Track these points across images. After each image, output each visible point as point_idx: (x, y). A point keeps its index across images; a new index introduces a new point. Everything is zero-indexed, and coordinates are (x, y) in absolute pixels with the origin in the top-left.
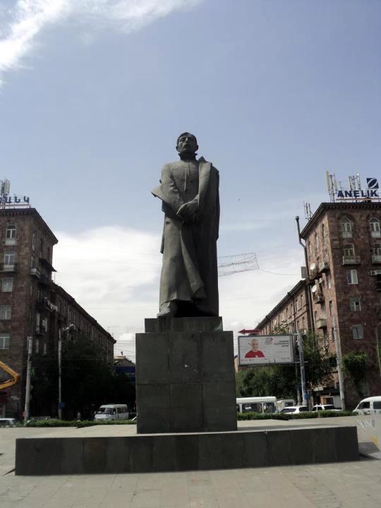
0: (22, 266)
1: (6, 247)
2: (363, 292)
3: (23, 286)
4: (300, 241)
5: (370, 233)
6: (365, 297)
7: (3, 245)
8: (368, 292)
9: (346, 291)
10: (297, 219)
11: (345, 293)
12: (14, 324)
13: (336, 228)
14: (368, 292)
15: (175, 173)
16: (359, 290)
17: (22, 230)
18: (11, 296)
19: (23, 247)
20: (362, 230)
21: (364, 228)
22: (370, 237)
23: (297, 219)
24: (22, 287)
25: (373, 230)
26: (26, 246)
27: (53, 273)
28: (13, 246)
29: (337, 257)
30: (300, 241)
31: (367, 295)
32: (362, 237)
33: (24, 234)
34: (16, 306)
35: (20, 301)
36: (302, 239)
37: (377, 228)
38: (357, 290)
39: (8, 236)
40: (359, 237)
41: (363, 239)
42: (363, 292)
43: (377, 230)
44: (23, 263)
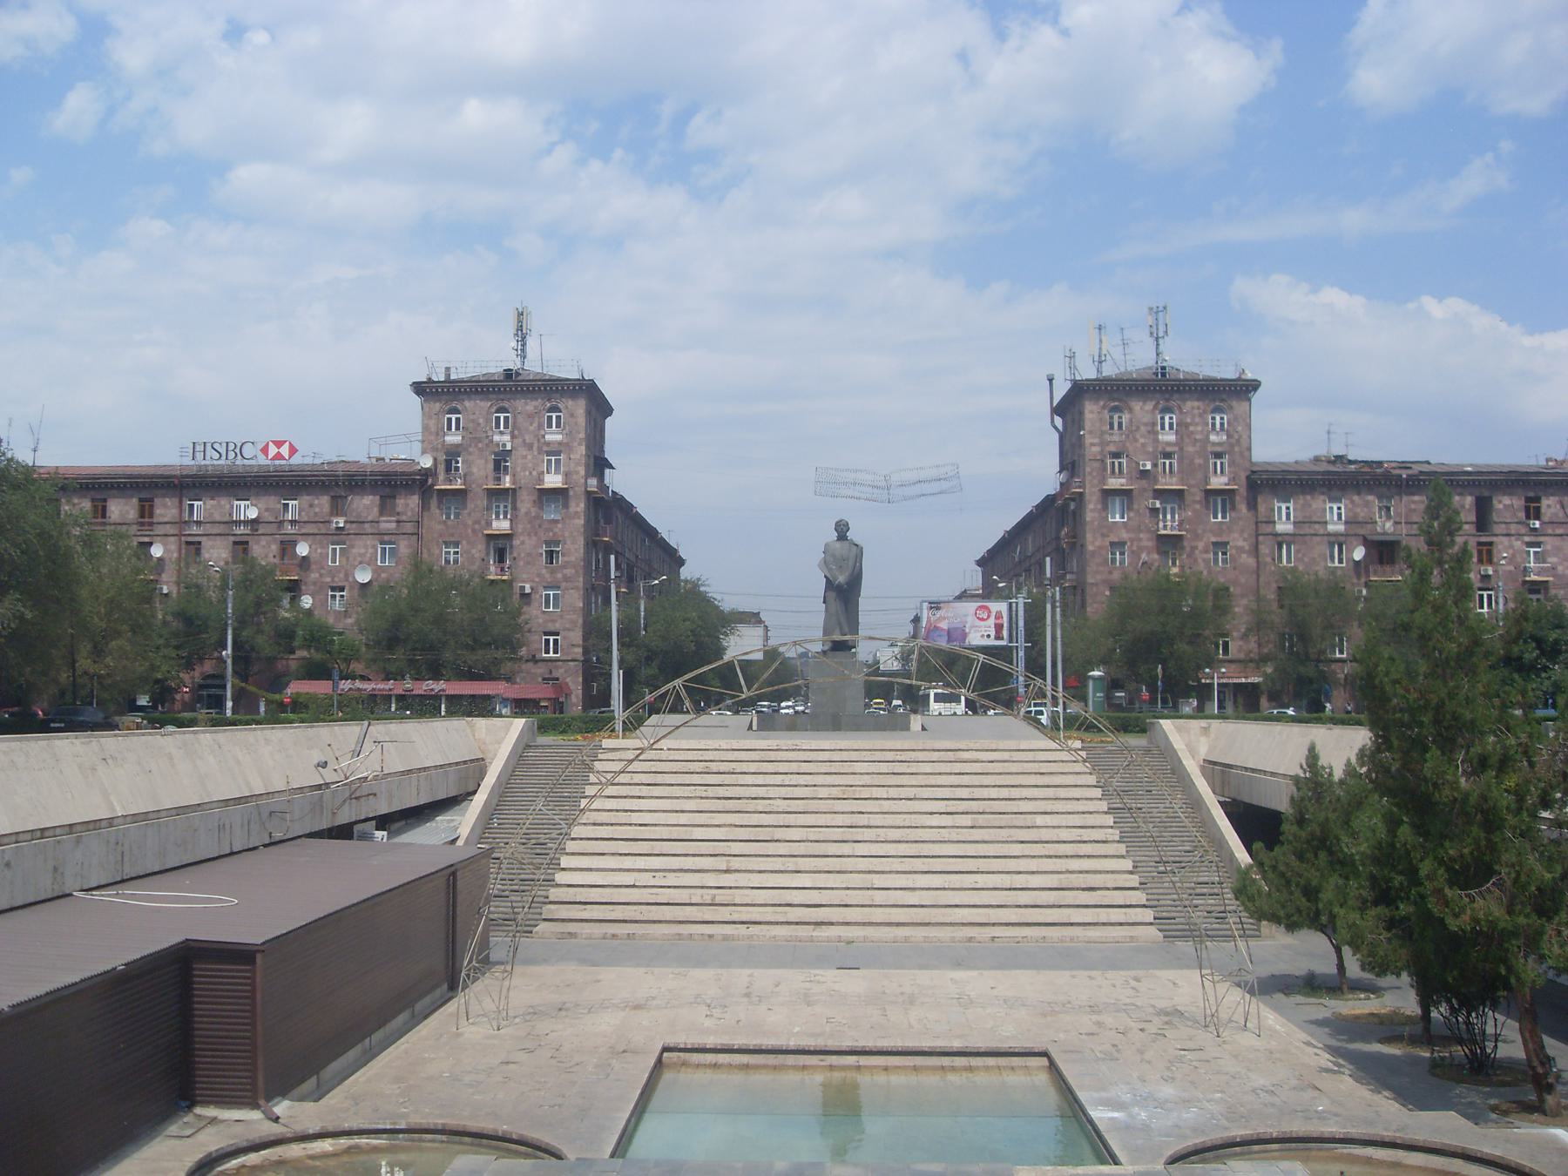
0: (575, 477)
1: (548, 444)
2: (1132, 535)
3: (579, 509)
4: (1052, 421)
5: (1156, 433)
6: (1135, 544)
7: (542, 440)
8: (1141, 535)
9: (1105, 531)
10: (1051, 380)
11: (1103, 535)
12: (565, 571)
13: (1098, 424)
14: (1141, 535)
16: (1128, 532)
17: (572, 415)
18: (560, 526)
19: (576, 444)
20: (1142, 428)
21: (1146, 424)
22: (1156, 441)
23: (1051, 380)
24: (577, 512)
25: (1163, 428)
26: (580, 444)
27: (607, 471)
28: (560, 443)
29: (1095, 474)
30: (1052, 421)
31: (1140, 540)
32: (1142, 440)
33: (576, 423)
34: (568, 542)
35: (575, 534)
37: (1171, 425)
38: (1123, 531)
39: (550, 426)
40: (1136, 440)
41: (1143, 445)
42: (1132, 535)
43: (1171, 427)
44: (577, 473)
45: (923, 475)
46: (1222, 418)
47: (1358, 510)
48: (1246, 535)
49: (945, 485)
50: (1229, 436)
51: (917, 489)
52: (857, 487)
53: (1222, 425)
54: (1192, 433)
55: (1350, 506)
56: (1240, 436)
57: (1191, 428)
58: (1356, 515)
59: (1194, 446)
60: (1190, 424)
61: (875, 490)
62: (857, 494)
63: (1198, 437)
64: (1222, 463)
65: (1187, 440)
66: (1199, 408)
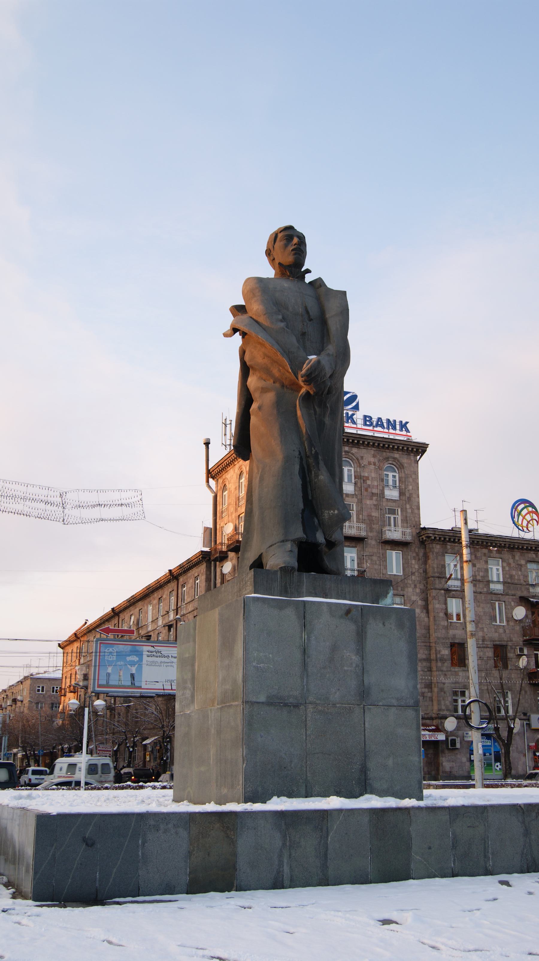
4: (208, 481)
10: (207, 444)
15: (264, 313)
23: (207, 444)
30: (208, 481)
36: (211, 480)
45: (103, 498)
46: (394, 477)
47: (514, 573)
48: (418, 590)
49: (126, 511)
50: (401, 494)
51: (96, 513)
52: (28, 503)
53: (395, 482)
54: (369, 485)
55: (507, 569)
56: (411, 494)
57: (369, 482)
58: (511, 576)
59: (371, 499)
60: (367, 478)
61: (48, 507)
62: (26, 510)
63: (375, 491)
64: (395, 518)
65: (364, 493)
66: (375, 464)
